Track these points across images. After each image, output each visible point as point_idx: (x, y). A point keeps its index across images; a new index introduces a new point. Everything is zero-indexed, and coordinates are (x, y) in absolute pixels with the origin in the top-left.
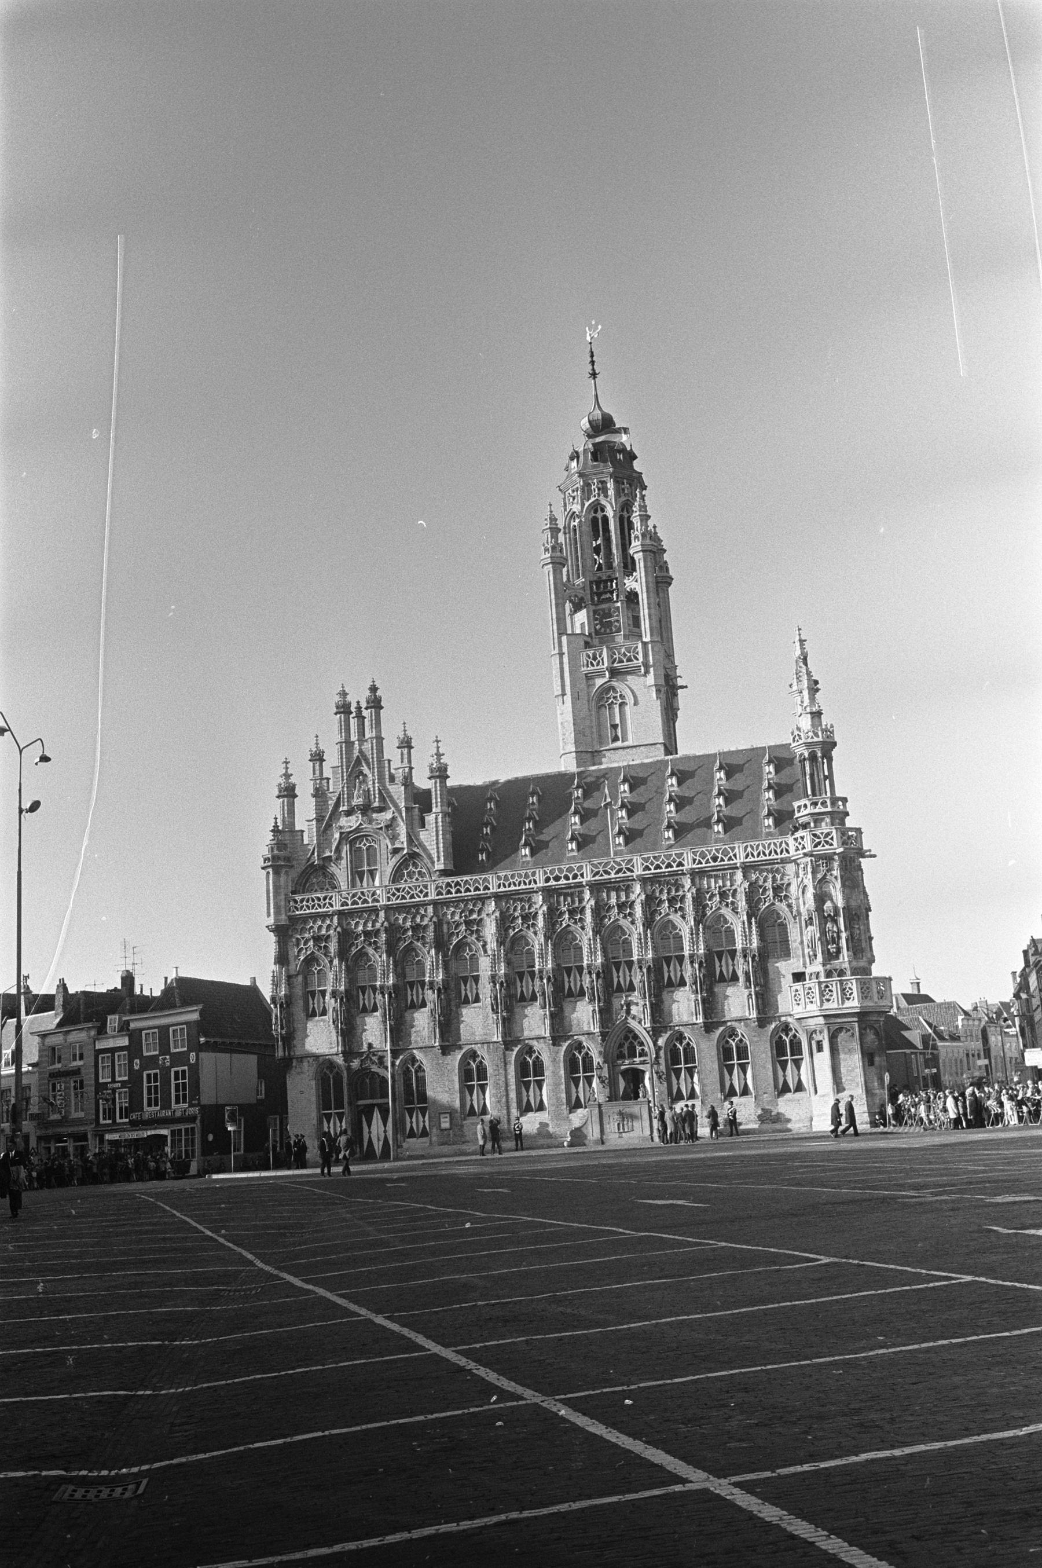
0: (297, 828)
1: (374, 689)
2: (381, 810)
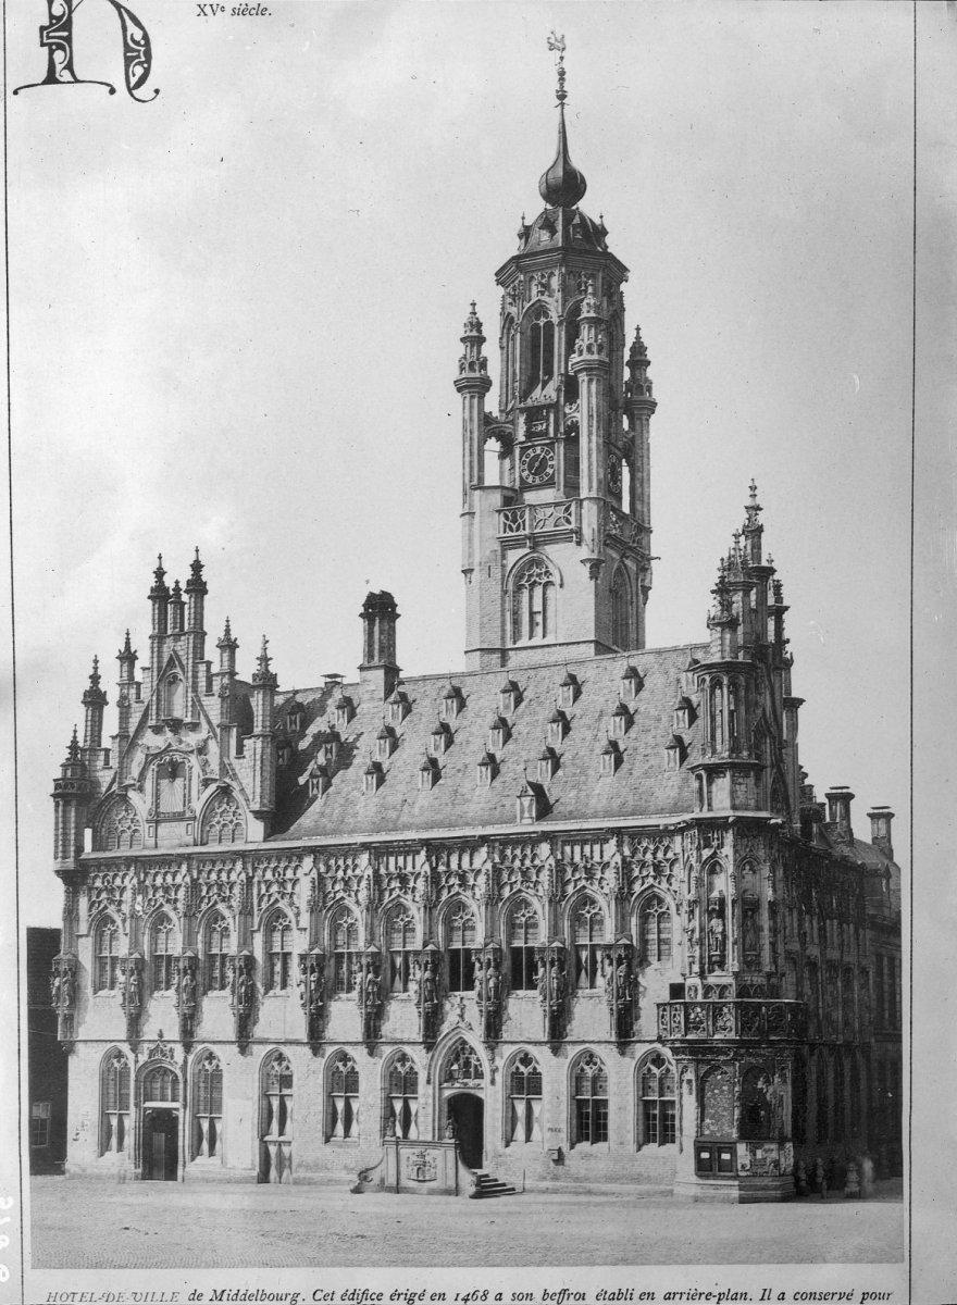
0: (103, 746)
1: (197, 567)
2: (195, 727)
